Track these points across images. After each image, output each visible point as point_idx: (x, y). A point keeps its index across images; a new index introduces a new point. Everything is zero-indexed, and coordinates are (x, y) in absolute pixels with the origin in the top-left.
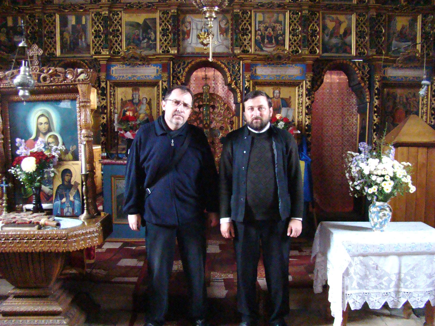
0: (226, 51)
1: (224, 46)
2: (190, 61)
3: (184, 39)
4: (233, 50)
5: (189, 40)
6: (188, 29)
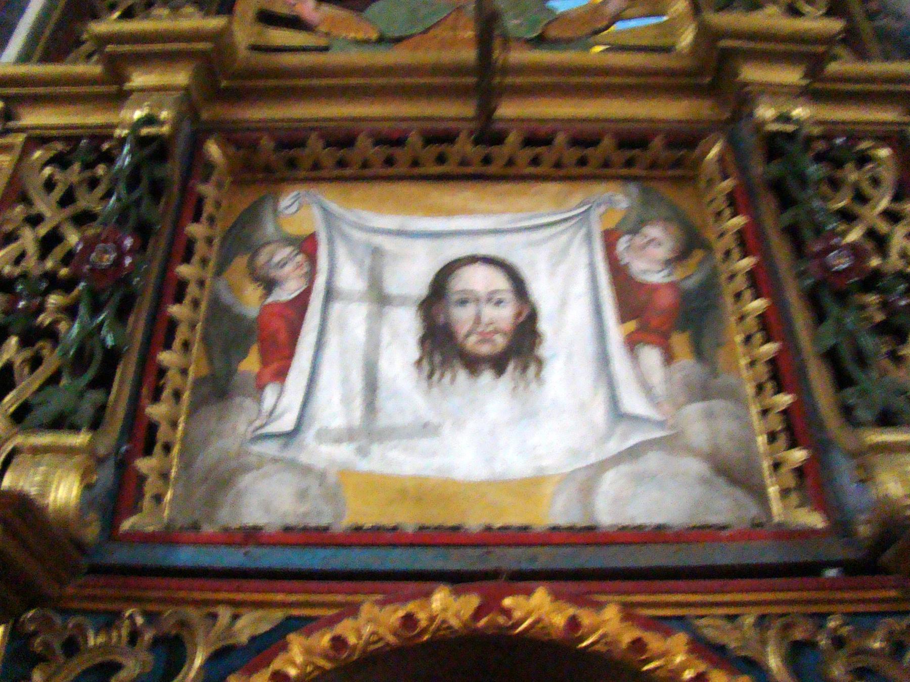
0: (725, 508)
1: (695, 467)
2: (249, 626)
3: (218, 390)
4: (811, 483)
5: (284, 402)
6: (287, 292)
